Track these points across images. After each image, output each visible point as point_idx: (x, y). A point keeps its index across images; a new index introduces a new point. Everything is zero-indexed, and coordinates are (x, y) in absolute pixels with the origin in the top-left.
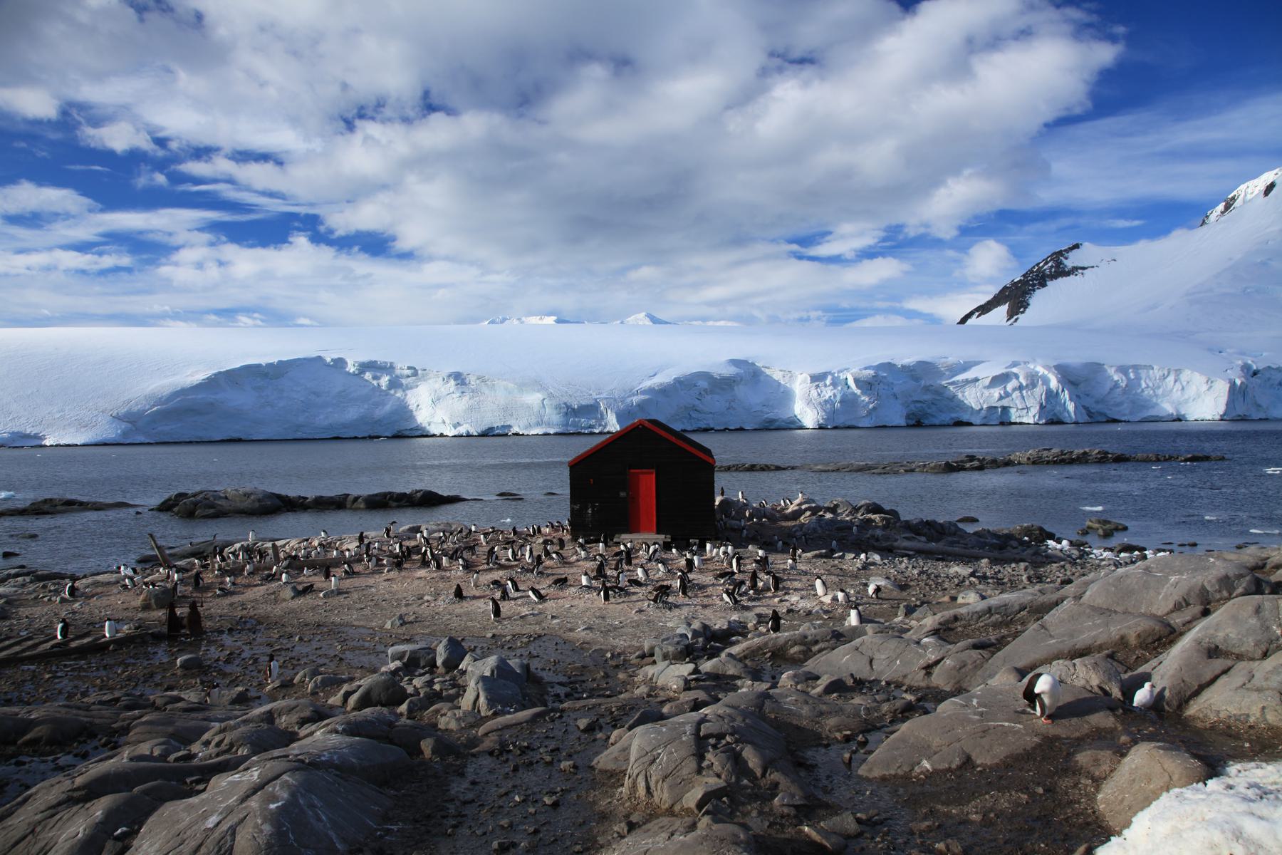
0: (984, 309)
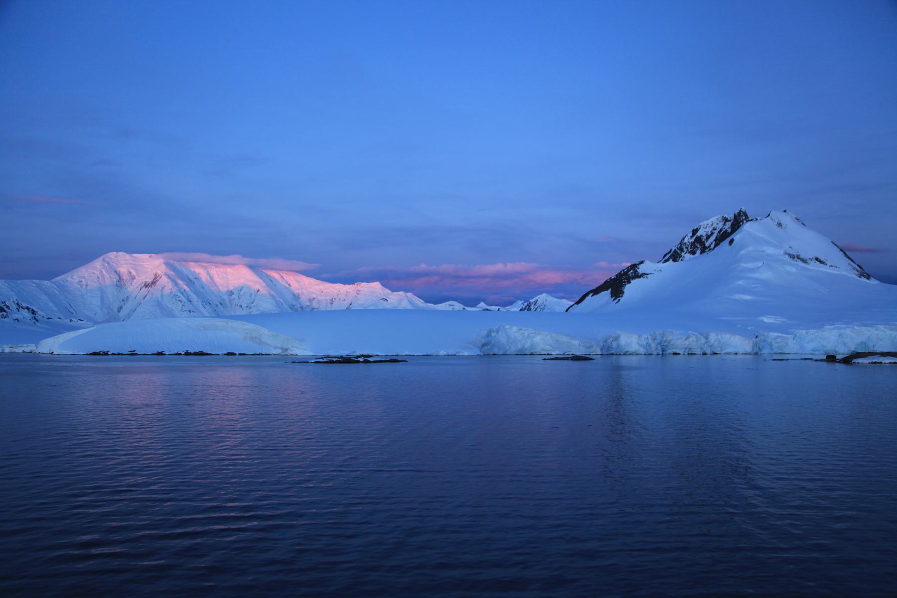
0: (596, 291)
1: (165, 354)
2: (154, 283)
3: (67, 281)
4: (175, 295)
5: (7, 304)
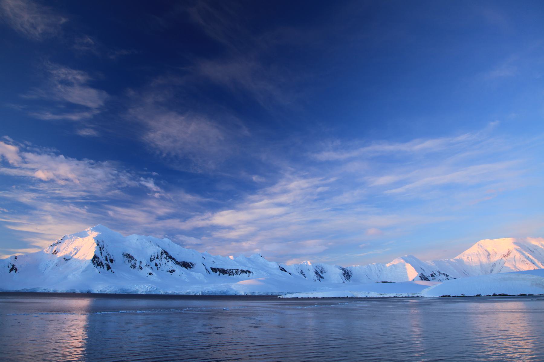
1: (481, 296)
2: (508, 254)
3: (461, 258)
4: (523, 260)
5: (435, 273)
